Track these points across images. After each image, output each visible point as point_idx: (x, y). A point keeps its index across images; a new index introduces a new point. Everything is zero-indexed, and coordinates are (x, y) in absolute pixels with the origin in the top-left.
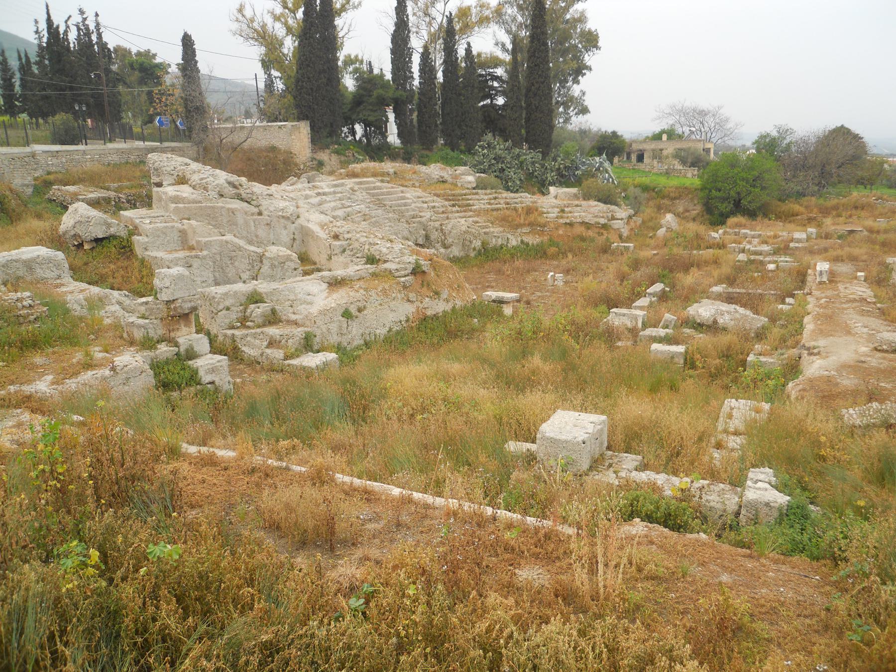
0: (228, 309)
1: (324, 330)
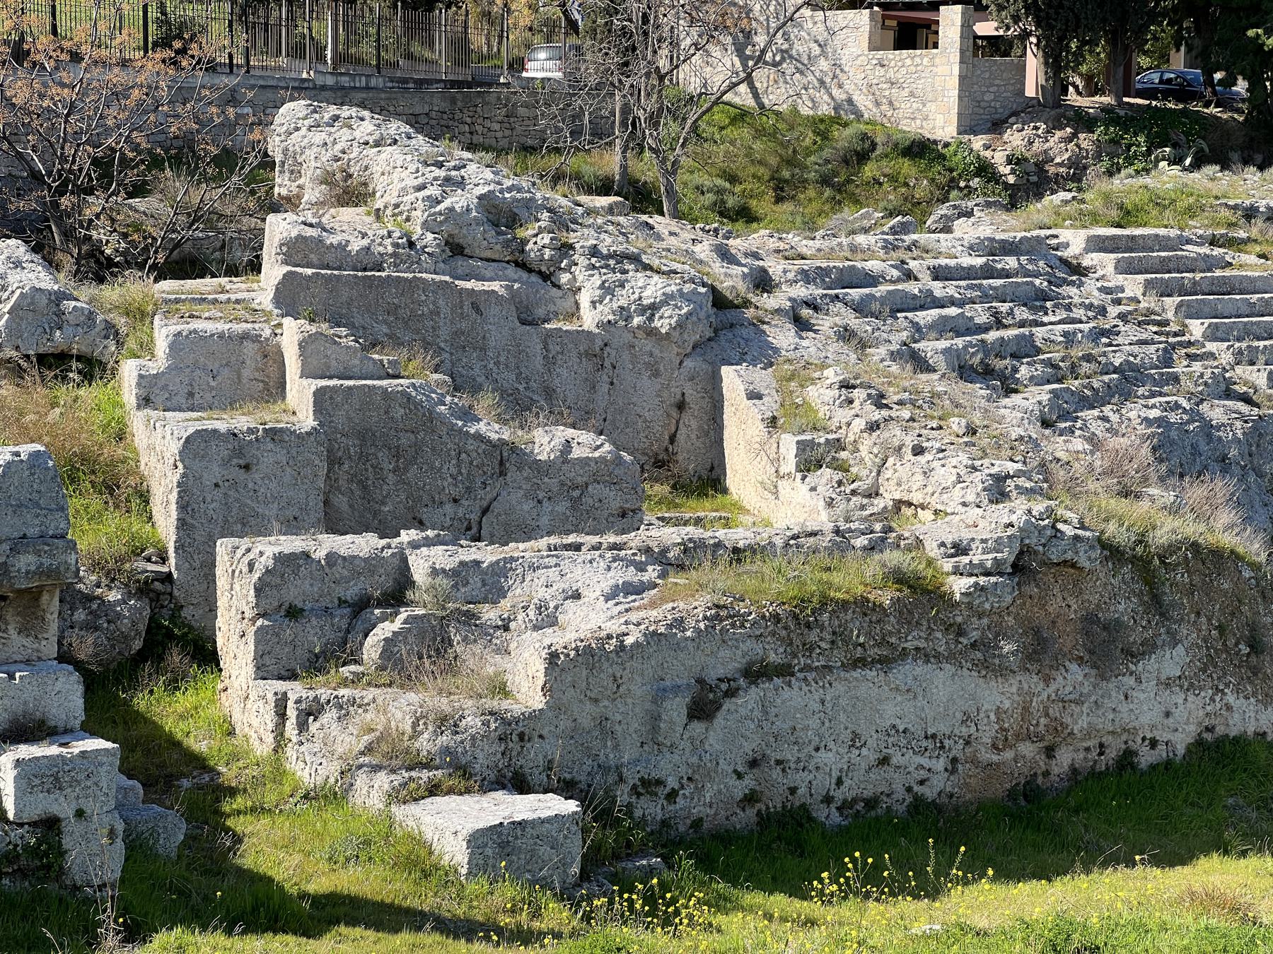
1: (586, 722)
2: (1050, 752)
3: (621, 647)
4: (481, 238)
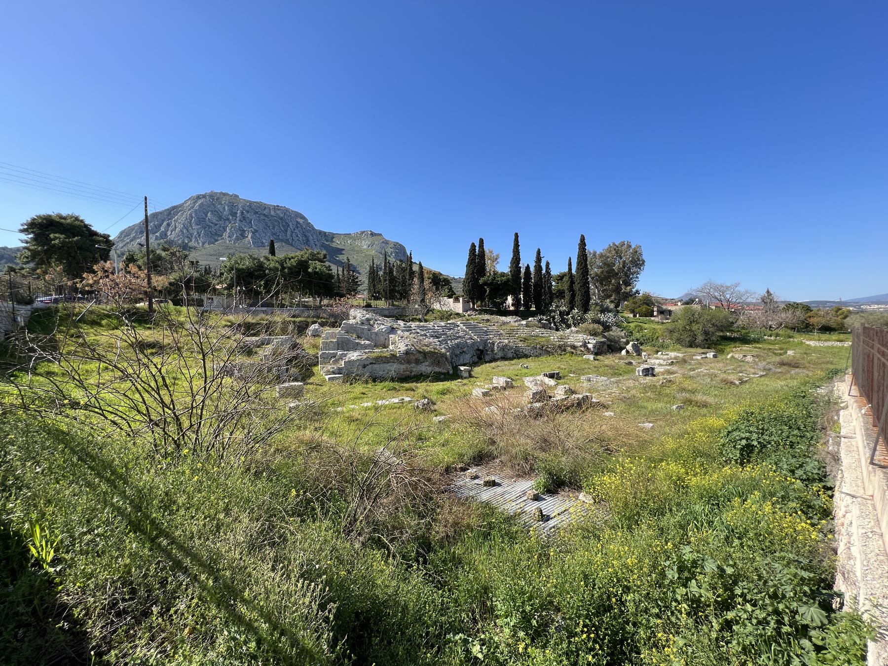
4: (365, 322)
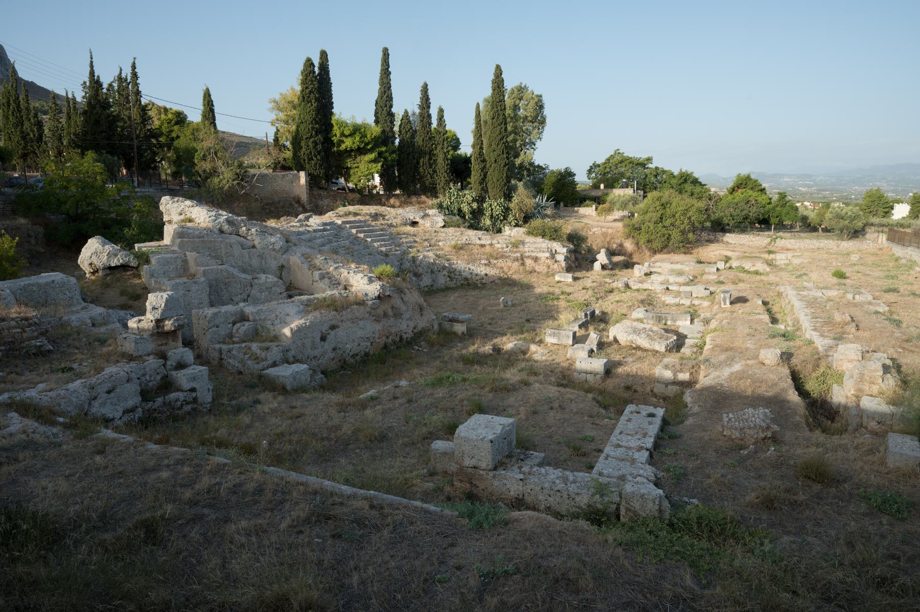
0: (217, 327)
2: (388, 337)
3: (306, 326)
